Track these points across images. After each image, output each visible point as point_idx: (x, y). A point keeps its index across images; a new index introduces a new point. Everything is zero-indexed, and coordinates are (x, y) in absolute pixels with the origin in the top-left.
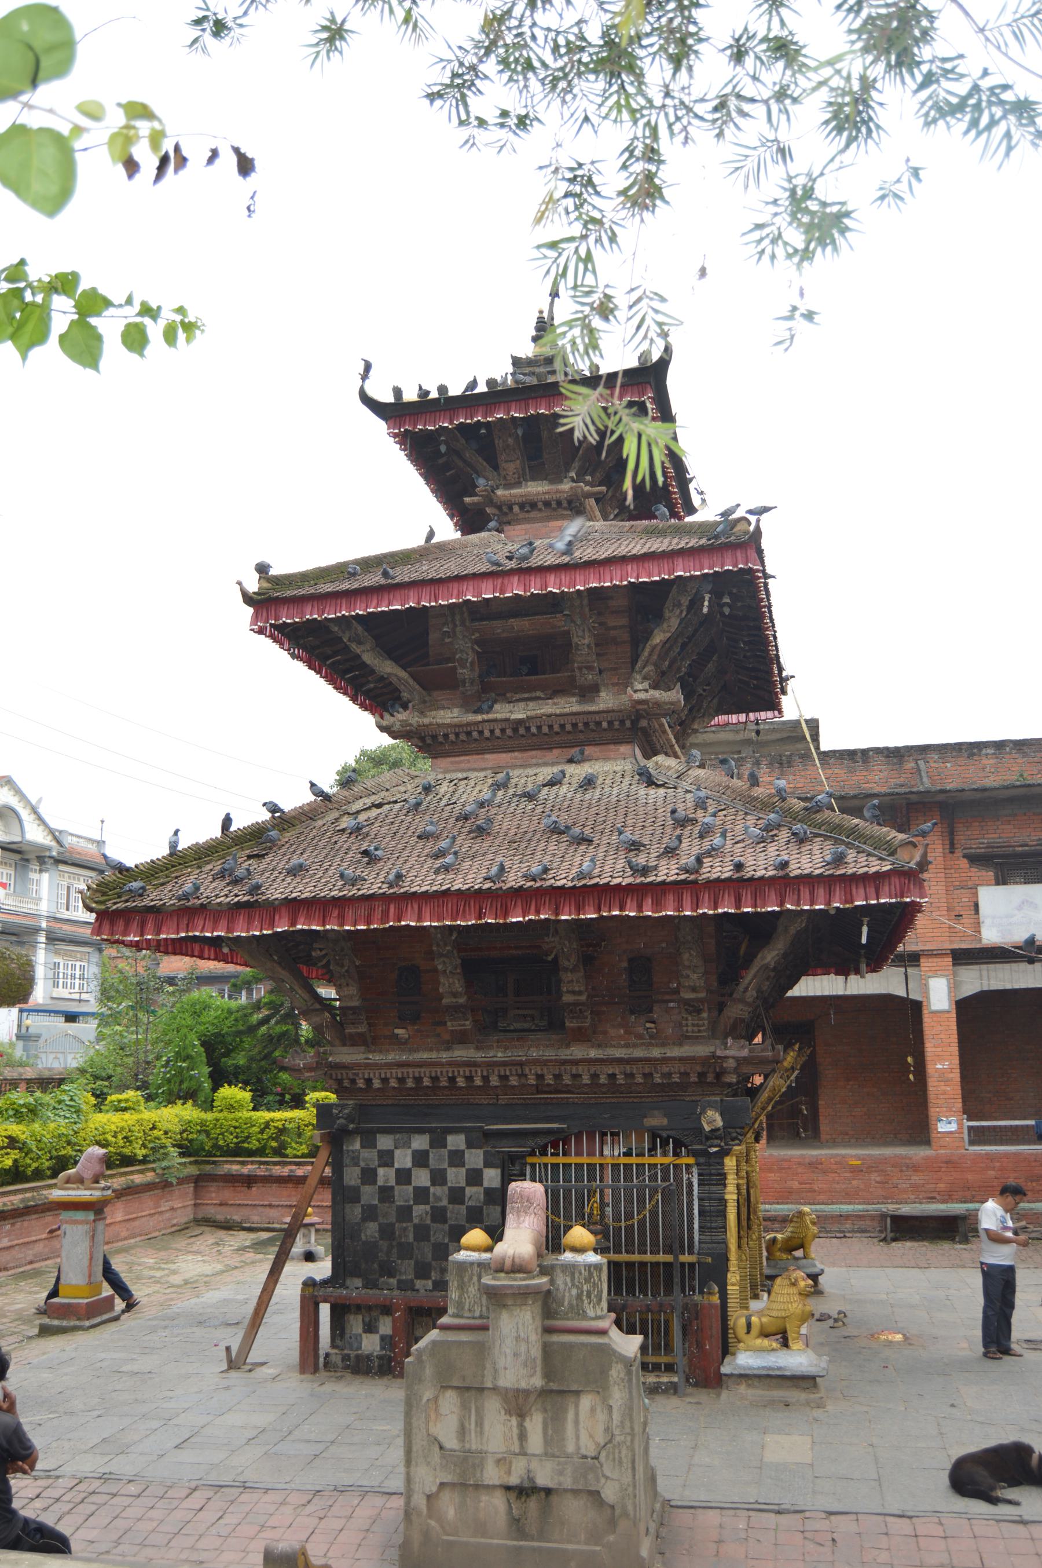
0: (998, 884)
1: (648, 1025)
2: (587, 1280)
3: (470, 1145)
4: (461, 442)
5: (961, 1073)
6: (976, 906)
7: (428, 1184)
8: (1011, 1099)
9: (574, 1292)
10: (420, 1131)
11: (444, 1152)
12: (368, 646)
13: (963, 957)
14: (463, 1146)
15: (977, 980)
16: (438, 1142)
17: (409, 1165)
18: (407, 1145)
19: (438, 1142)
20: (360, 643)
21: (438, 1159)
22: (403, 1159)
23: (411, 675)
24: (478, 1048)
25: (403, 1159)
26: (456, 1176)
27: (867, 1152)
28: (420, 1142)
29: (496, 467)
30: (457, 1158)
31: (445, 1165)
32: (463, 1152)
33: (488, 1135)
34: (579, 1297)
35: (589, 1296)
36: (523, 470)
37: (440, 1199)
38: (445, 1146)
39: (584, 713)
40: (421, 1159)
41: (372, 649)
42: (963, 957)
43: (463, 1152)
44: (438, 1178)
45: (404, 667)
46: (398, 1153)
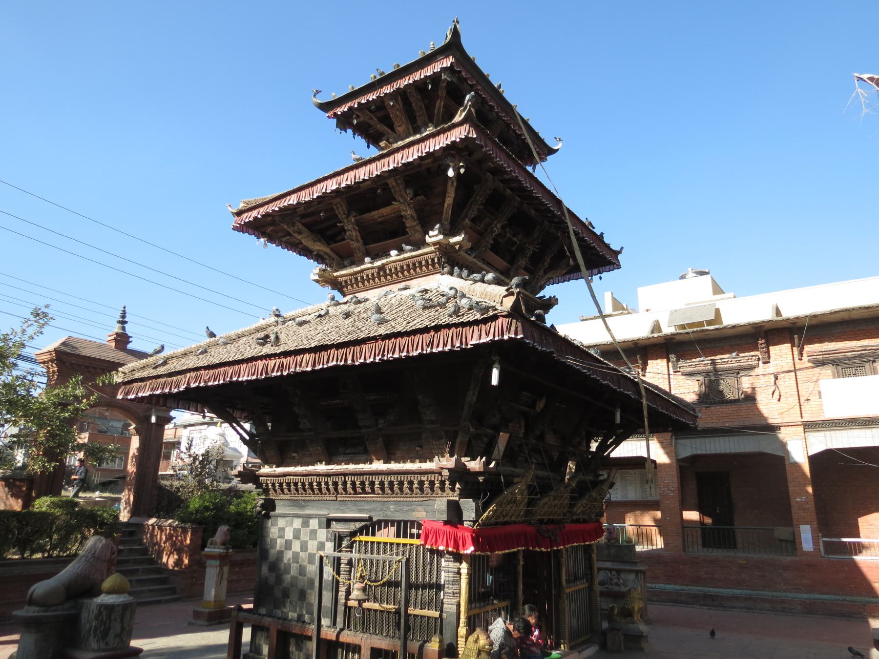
0: (834, 377)
1: (417, 449)
2: (96, 618)
3: (320, 527)
4: (369, 116)
5: (816, 504)
6: (820, 393)
7: (299, 550)
8: (872, 525)
9: (88, 626)
10: (298, 516)
11: (308, 530)
12: (304, 235)
13: (810, 426)
14: (317, 527)
15: (820, 442)
16: (305, 524)
17: (291, 538)
18: (292, 523)
19: (305, 524)
20: (300, 233)
21: (305, 535)
22: (289, 535)
23: (332, 250)
24: (327, 464)
25: (289, 535)
26: (312, 546)
27: (766, 557)
28: (297, 523)
29: (393, 129)
30: (313, 533)
31: (307, 539)
32: (316, 531)
33: (329, 522)
34: (90, 629)
35: (95, 631)
36: (408, 129)
37: (303, 561)
38: (308, 526)
39: (412, 257)
40: (297, 535)
41: (308, 237)
42: (810, 426)
43: (316, 531)
44: (304, 547)
45: (329, 244)
46: (287, 529)
